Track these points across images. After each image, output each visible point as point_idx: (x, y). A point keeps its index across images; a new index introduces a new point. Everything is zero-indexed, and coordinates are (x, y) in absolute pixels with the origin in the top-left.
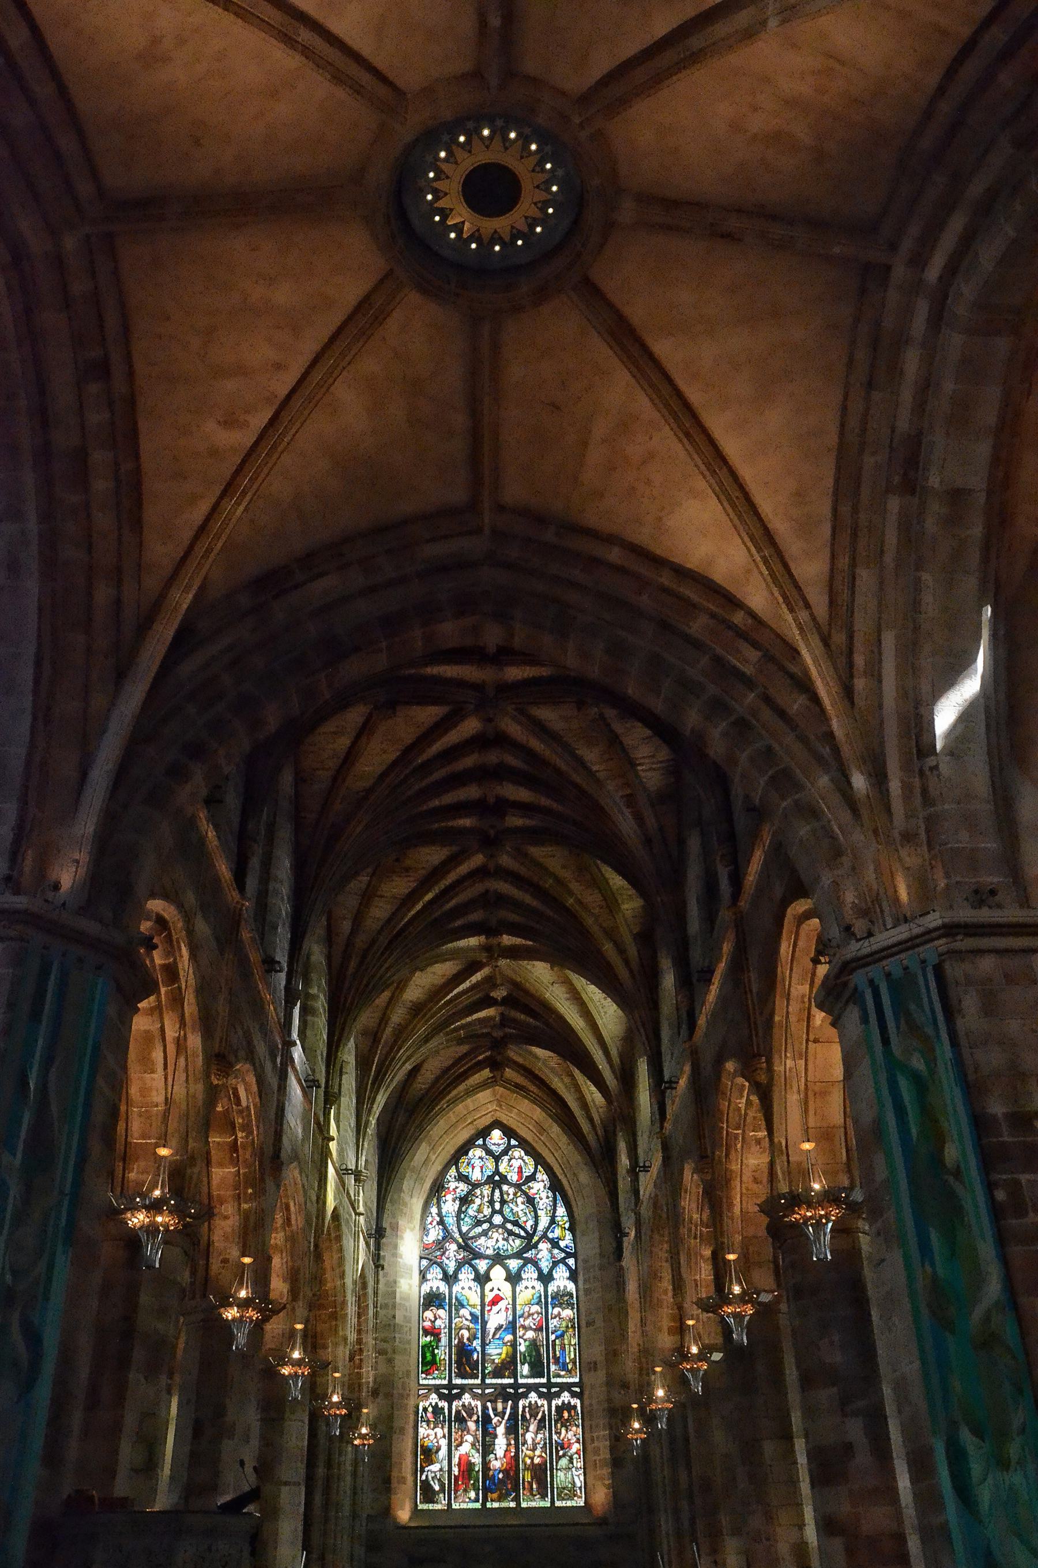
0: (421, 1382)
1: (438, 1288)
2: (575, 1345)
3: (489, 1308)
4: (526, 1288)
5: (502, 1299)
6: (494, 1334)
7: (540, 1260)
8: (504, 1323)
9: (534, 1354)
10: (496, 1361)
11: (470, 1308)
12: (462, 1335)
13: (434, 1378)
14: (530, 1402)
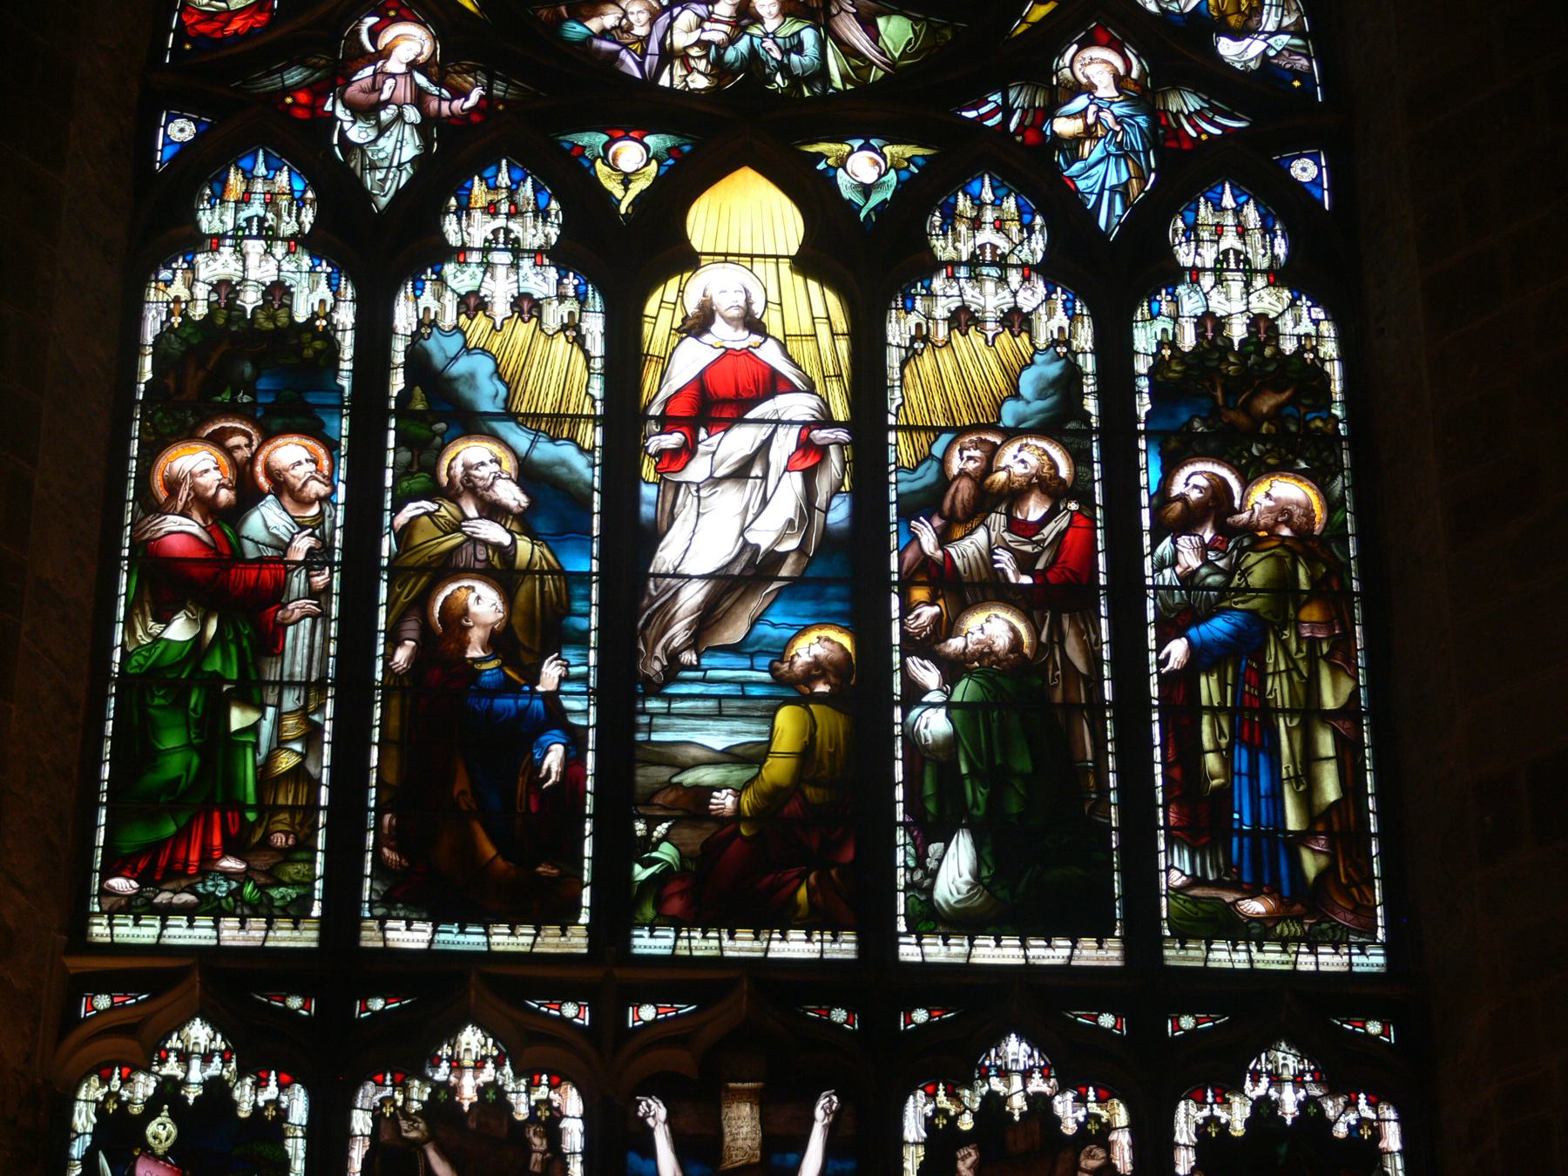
0: (100, 931)
1: (277, 292)
2: (1349, 710)
3: (673, 440)
4: (963, 319)
5: (774, 384)
6: (708, 618)
7: (1071, 147)
8: (791, 544)
9: (1024, 764)
10: (724, 801)
11: (520, 439)
12: (456, 618)
13: (216, 910)
14: (995, 1103)
